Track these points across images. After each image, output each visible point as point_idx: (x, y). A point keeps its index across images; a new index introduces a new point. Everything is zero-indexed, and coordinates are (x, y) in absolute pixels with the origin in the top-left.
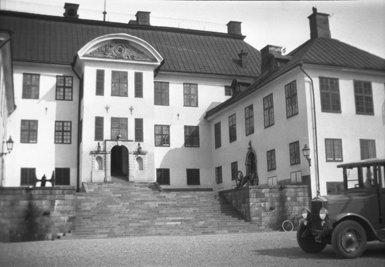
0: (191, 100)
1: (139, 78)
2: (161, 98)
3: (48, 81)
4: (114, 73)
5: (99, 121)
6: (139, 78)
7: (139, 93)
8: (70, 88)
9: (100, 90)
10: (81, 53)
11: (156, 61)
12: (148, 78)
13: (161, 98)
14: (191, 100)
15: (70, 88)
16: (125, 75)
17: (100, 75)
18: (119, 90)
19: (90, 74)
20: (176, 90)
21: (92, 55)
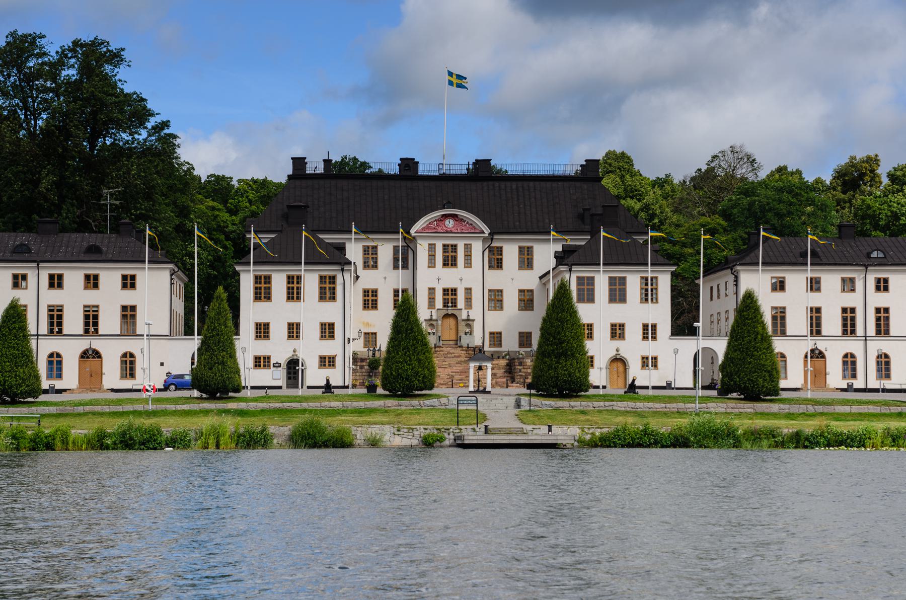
0: (526, 261)
1: (468, 248)
3: (385, 252)
4: (444, 245)
5: (432, 291)
6: (468, 248)
7: (468, 263)
8: (404, 259)
9: (432, 263)
11: (483, 233)
12: (478, 247)
14: (526, 261)
15: (404, 259)
16: (454, 247)
17: (432, 247)
18: (450, 262)
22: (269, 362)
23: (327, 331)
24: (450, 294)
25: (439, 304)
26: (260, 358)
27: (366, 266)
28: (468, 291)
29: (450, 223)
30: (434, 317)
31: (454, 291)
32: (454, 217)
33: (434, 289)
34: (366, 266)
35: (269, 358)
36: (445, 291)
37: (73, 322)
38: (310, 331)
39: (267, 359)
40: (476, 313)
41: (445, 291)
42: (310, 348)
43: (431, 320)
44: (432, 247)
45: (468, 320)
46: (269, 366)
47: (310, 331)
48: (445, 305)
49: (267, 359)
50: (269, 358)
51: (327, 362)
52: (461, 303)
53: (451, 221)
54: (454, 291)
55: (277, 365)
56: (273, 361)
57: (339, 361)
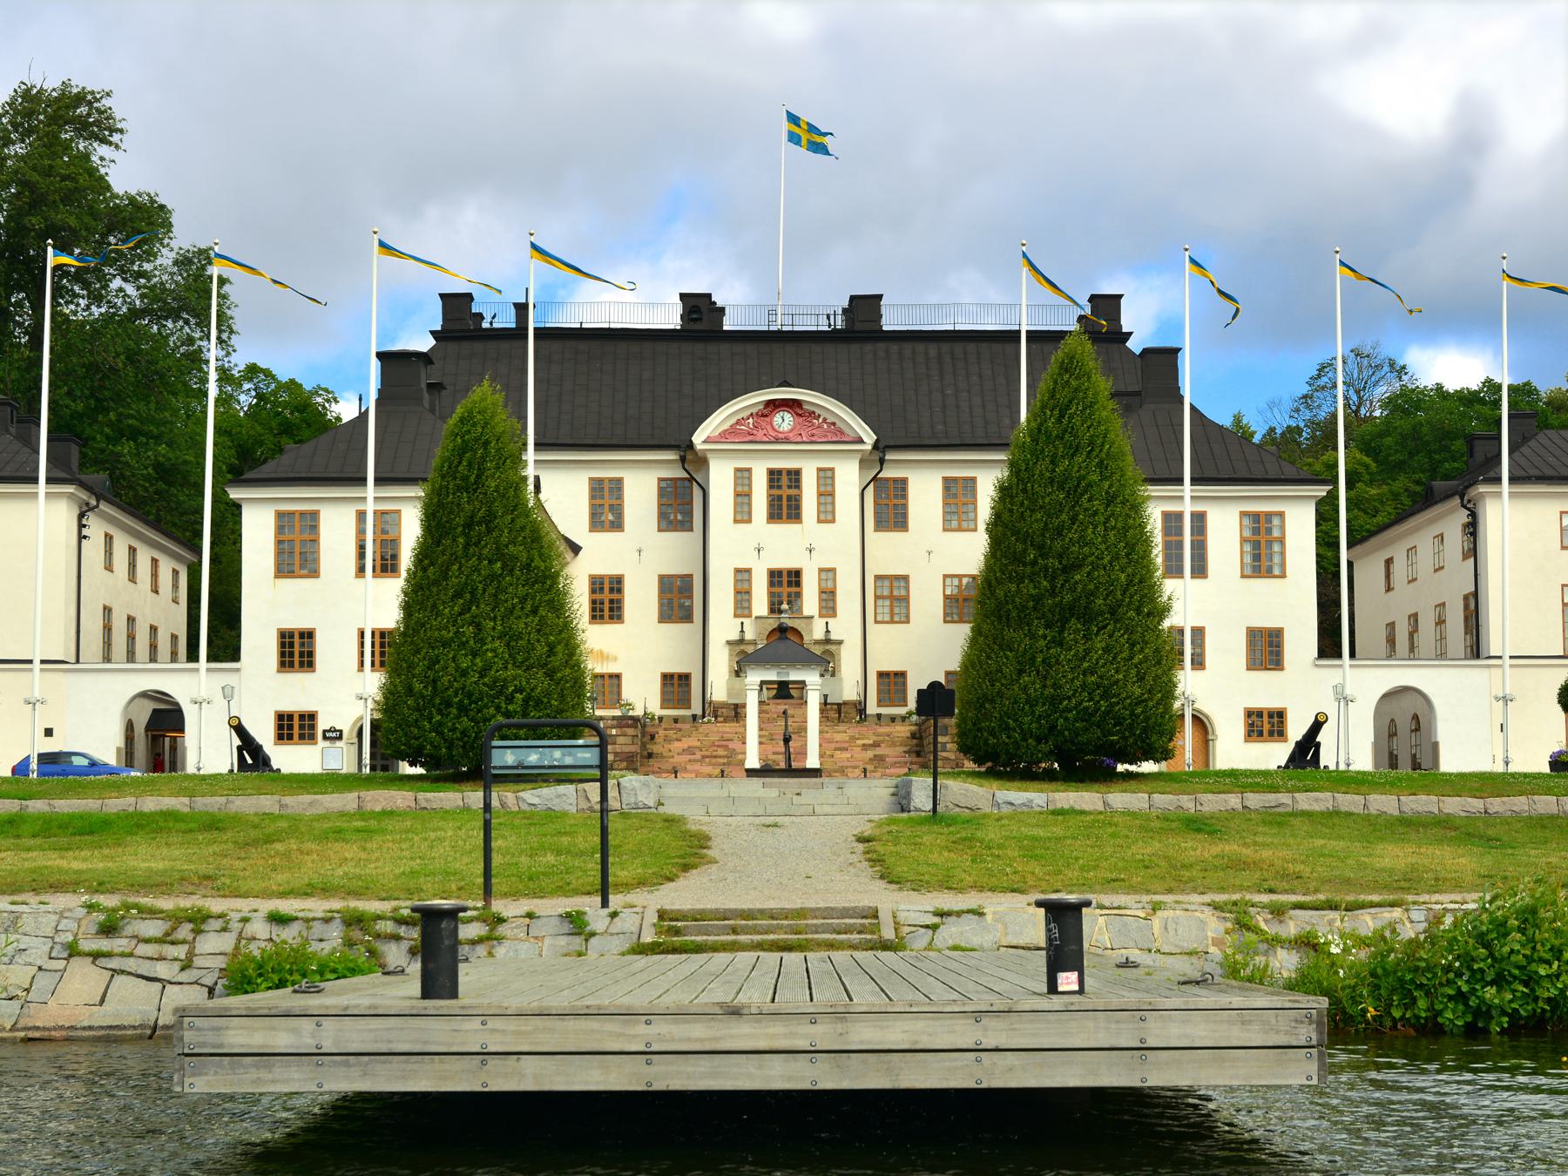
1: (826, 478)
2: (890, 510)
4: (771, 472)
5: (743, 576)
7: (827, 515)
9: (743, 514)
10: (698, 439)
11: (861, 441)
12: (849, 477)
13: (890, 510)
15: (681, 506)
16: (795, 476)
17: (743, 476)
18: (785, 508)
19: (720, 477)
20: (925, 488)
21: (725, 436)
22: (313, 727)
24: (786, 582)
25: (760, 605)
26: (290, 717)
27: (597, 524)
28: (828, 573)
29: (784, 421)
30: (749, 636)
31: (795, 576)
32: (792, 405)
33: (749, 571)
34: (597, 524)
35: (312, 716)
36: (775, 576)
39: (309, 718)
40: (846, 626)
41: (775, 576)
43: (742, 641)
44: (743, 476)
45: (828, 641)
48: (775, 608)
49: (309, 718)
50: (312, 716)
52: (810, 602)
53: (787, 416)
54: (795, 576)
55: (334, 735)
56: (322, 724)
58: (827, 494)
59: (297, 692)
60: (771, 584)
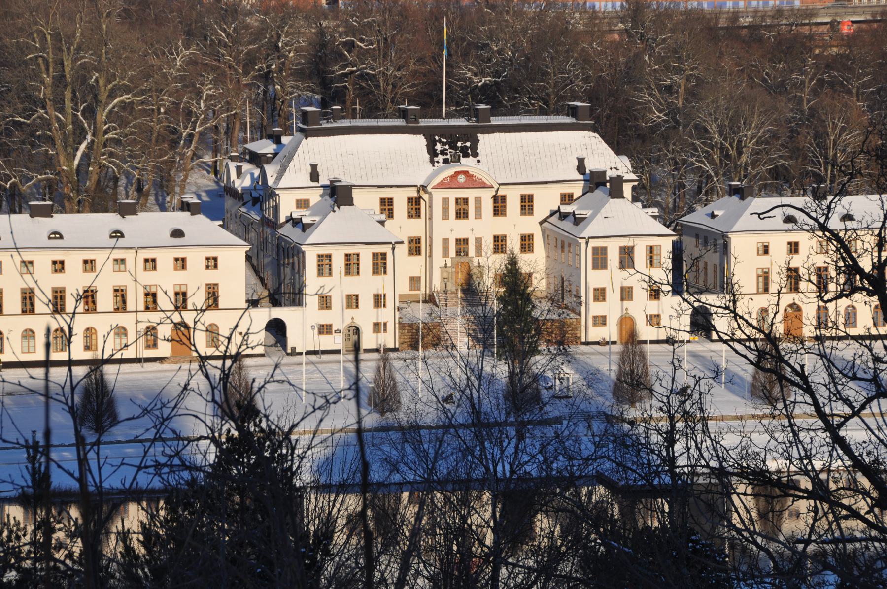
1: (478, 201)
5: (446, 241)
9: (446, 216)
16: (466, 201)
17: (446, 201)
18: (462, 214)
22: (331, 329)
23: (379, 301)
24: (462, 243)
25: (452, 252)
28: (479, 241)
30: (449, 265)
31: (466, 241)
35: (331, 325)
36: (458, 241)
37: (105, 300)
38: (366, 301)
41: (458, 241)
42: (365, 316)
46: (331, 333)
47: (366, 301)
48: (458, 253)
49: (329, 327)
50: (331, 325)
51: (377, 327)
52: (472, 251)
54: (466, 241)
55: (338, 331)
56: (334, 329)
57: (390, 327)
58: (478, 208)
59: (325, 317)
60: (457, 244)
